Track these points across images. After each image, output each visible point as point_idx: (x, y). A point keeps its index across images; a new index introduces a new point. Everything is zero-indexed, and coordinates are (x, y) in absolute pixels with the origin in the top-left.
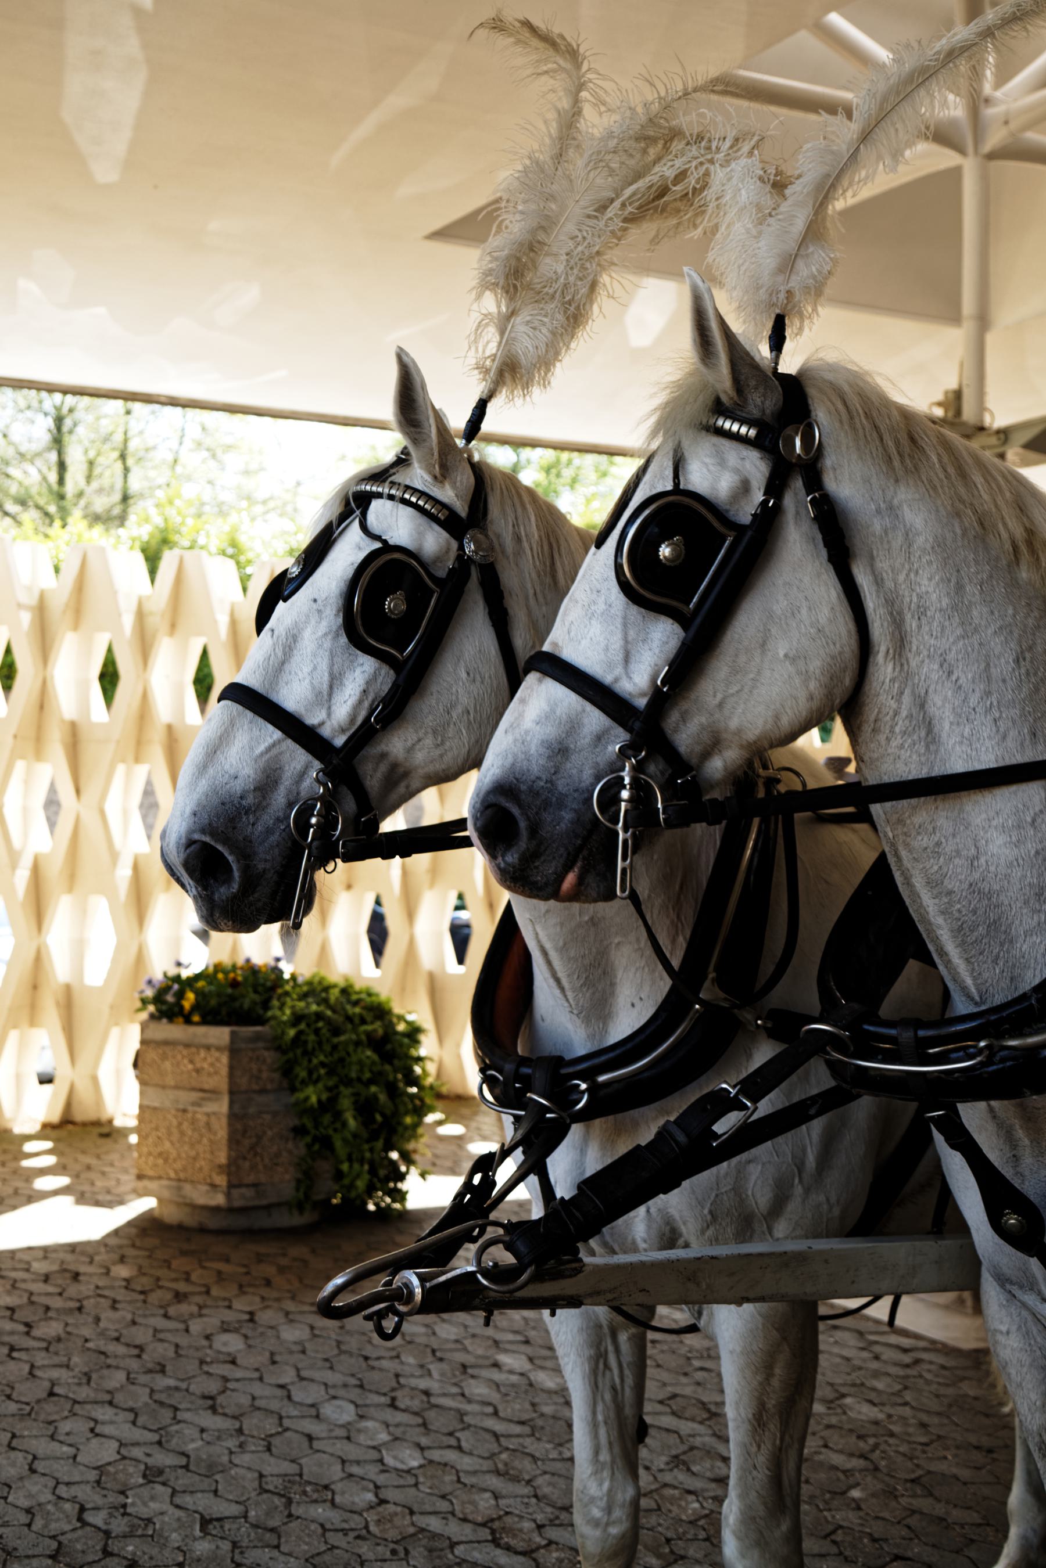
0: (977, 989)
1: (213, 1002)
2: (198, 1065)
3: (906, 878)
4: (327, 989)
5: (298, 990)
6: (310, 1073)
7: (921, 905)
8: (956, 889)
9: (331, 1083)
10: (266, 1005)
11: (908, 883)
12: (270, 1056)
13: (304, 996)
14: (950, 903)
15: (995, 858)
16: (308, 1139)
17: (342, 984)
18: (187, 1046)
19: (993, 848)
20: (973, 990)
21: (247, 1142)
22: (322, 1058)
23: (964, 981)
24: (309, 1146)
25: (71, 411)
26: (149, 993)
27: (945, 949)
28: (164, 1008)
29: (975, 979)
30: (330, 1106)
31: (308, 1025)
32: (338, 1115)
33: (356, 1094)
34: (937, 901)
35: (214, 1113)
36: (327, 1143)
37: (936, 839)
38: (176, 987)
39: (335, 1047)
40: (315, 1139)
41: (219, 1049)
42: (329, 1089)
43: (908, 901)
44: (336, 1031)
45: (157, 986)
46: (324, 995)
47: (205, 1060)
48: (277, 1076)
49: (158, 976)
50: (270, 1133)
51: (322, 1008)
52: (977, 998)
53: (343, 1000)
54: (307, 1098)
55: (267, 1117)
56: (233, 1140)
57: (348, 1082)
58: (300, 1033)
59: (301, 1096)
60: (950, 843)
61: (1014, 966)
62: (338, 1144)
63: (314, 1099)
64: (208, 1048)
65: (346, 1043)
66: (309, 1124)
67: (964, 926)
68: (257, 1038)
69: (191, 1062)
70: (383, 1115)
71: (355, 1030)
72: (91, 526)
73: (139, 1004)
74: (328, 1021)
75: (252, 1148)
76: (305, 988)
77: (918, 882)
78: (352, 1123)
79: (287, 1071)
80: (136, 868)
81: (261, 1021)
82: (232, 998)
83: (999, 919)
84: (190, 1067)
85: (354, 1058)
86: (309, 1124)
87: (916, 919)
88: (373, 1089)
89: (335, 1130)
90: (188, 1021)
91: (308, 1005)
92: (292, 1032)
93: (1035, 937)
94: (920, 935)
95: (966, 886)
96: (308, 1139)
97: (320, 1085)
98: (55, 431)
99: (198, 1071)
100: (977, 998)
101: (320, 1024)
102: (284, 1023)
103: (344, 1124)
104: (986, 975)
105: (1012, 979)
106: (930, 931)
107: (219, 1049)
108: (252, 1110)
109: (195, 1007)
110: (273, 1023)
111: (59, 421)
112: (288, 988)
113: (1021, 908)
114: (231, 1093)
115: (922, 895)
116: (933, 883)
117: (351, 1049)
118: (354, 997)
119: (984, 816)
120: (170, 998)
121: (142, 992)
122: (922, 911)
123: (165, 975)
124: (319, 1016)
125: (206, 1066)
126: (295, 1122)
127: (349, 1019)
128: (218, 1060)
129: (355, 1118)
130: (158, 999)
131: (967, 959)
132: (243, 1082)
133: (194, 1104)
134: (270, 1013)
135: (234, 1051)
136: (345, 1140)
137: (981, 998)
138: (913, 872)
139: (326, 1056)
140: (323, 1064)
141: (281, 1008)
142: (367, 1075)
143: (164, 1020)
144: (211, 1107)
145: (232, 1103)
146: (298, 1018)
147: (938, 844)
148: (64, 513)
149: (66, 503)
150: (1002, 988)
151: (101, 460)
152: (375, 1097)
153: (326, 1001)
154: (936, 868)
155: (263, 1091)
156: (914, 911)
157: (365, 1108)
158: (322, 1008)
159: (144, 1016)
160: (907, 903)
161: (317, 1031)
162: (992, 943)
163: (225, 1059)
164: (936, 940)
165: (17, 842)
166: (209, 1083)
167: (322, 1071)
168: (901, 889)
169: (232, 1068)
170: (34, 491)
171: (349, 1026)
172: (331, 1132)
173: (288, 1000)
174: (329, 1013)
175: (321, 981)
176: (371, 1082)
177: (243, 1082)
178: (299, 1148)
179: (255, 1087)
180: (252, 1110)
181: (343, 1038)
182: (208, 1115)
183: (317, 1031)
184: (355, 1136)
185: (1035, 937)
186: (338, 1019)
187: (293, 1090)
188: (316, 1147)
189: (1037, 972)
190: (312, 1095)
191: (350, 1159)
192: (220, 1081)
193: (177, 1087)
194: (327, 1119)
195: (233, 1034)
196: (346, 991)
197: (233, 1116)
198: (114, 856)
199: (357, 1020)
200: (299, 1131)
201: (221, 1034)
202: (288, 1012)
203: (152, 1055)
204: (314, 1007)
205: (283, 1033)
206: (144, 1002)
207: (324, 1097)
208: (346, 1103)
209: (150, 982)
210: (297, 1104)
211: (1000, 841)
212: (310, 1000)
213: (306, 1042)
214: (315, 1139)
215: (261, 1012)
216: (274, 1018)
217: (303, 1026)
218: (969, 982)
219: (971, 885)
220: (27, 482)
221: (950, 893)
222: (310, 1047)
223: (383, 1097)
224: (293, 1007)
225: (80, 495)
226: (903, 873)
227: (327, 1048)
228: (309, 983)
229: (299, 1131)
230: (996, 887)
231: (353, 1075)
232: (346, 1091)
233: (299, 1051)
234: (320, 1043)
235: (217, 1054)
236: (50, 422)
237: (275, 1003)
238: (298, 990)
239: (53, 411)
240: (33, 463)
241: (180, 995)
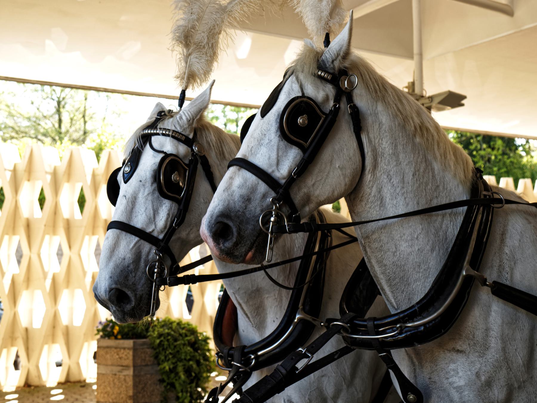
0: (396, 303)
1: (126, 330)
2: (121, 356)
3: (368, 260)
4: (171, 323)
5: (160, 324)
6: (166, 357)
7: (375, 271)
8: (388, 264)
9: (174, 361)
10: (147, 330)
11: (370, 262)
12: (149, 351)
13: (162, 326)
14: (385, 270)
15: (403, 252)
16: (165, 384)
17: (177, 321)
18: (116, 348)
19: (402, 248)
20: (394, 304)
21: (141, 386)
22: (170, 351)
23: (391, 301)
24: (165, 387)
25: (64, 99)
26: (100, 327)
27: (384, 288)
28: (106, 333)
29: (395, 299)
30: (173, 370)
31: (164, 338)
32: (177, 374)
33: (184, 365)
34: (380, 269)
35: (127, 375)
36: (173, 385)
37: (381, 245)
38: (111, 324)
39: (175, 347)
40: (168, 384)
41: (129, 349)
42: (173, 363)
43: (370, 269)
44: (176, 340)
45: (104, 324)
46: (170, 326)
47: (123, 354)
48: (152, 359)
49: (103, 320)
50: (150, 382)
51: (170, 331)
52: (396, 307)
53: (178, 327)
54: (165, 368)
55: (149, 376)
56: (135, 386)
57: (180, 360)
58: (161, 341)
59: (162, 366)
60: (386, 246)
61: (410, 294)
62: (177, 385)
63: (167, 368)
64: (124, 348)
65: (180, 345)
66: (165, 378)
67: (391, 278)
68: (144, 344)
69: (118, 354)
70: (195, 373)
71: (183, 339)
72: (72, 144)
73: (96, 332)
74: (172, 336)
75: (143, 388)
76: (163, 323)
77: (373, 261)
78: (183, 377)
79: (156, 357)
80: (93, 278)
81: (145, 337)
82: (134, 328)
83: (404, 276)
84: (117, 357)
85: (183, 351)
86: (165, 378)
87: (373, 276)
88: (191, 363)
89: (176, 380)
90: (116, 338)
91: (164, 330)
92: (158, 341)
93: (418, 283)
94: (375, 282)
95: (392, 263)
96: (165, 384)
97: (170, 362)
98: (57, 107)
99: (120, 358)
100: (396, 307)
101: (169, 337)
102: (155, 337)
103: (180, 377)
104: (399, 298)
105: (409, 299)
106: (378, 281)
107: (129, 349)
108: (142, 373)
109: (119, 332)
110: (150, 337)
111: (59, 103)
112: (156, 323)
113: (412, 271)
114: (134, 366)
115: (375, 266)
116: (379, 262)
117: (182, 347)
118: (182, 326)
119: (399, 236)
120: (109, 329)
121: (97, 327)
122: (375, 273)
123: (107, 319)
124: (169, 334)
125: (123, 356)
126: (159, 377)
127: (181, 335)
128: (128, 353)
129: (184, 375)
130: (104, 329)
131: (392, 292)
132: (139, 362)
133: (119, 372)
134: (149, 334)
135: (135, 349)
136: (180, 384)
137: (397, 307)
138: (372, 257)
139: (172, 350)
140: (171, 354)
141: (154, 331)
142: (188, 357)
143: (107, 338)
144: (126, 373)
145: (134, 371)
146: (160, 335)
147: (381, 246)
148: (61, 139)
149: (62, 135)
150: (405, 303)
151: (75, 118)
152: (192, 366)
153: (171, 328)
154: (380, 256)
155: (147, 365)
156: (372, 273)
157: (188, 371)
158: (170, 331)
159: (98, 337)
160: (370, 270)
161: (168, 340)
162: (401, 285)
163: (131, 353)
164: (380, 284)
165: (46, 270)
166: (125, 363)
167: (170, 356)
168: (367, 264)
169: (134, 356)
170: (49, 130)
171: (181, 338)
172: (174, 381)
173: (156, 328)
174: (172, 333)
175: (169, 320)
176: (190, 360)
177: (139, 362)
178: (161, 388)
179: (143, 364)
180: (142, 373)
181: (178, 343)
182: (125, 376)
183: (168, 340)
184: (184, 382)
185: (418, 283)
186: (176, 335)
187: (159, 364)
188: (169, 387)
189: (419, 296)
190: (167, 366)
191: (182, 391)
192: (129, 362)
193: (112, 365)
194: (173, 375)
195: (134, 342)
196: (179, 324)
197: (135, 376)
198: (85, 273)
199: (184, 335)
200: (162, 381)
201: (129, 343)
202: (156, 333)
203: (102, 352)
204: (166, 331)
205: (154, 342)
206: (98, 331)
207: (172, 366)
208: (180, 369)
209: (100, 323)
210: (161, 370)
211: (405, 245)
212: (165, 328)
213: (163, 345)
214: (168, 384)
215: (145, 333)
216: (150, 335)
217: (162, 338)
218: (393, 301)
219: (393, 262)
220: (46, 127)
221: (385, 265)
222: (165, 347)
223: (195, 366)
224: (158, 331)
225: (67, 131)
226: (368, 258)
227: (172, 347)
228: (164, 321)
229: (162, 381)
230: (403, 263)
231: (183, 357)
232: (180, 364)
233: (161, 349)
234: (169, 345)
235: (128, 351)
236: (56, 104)
237: (151, 329)
238: (160, 324)
239: (57, 99)
240: (49, 120)
241: (113, 328)
